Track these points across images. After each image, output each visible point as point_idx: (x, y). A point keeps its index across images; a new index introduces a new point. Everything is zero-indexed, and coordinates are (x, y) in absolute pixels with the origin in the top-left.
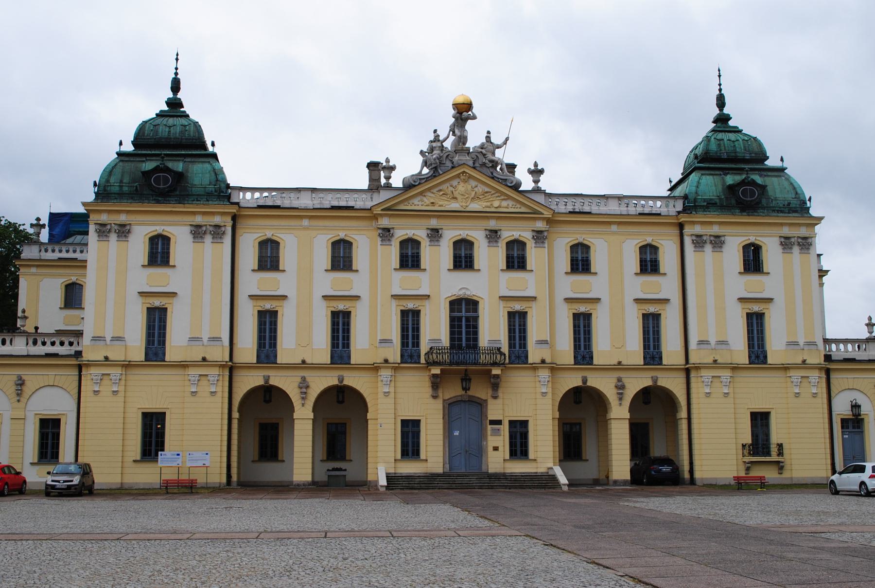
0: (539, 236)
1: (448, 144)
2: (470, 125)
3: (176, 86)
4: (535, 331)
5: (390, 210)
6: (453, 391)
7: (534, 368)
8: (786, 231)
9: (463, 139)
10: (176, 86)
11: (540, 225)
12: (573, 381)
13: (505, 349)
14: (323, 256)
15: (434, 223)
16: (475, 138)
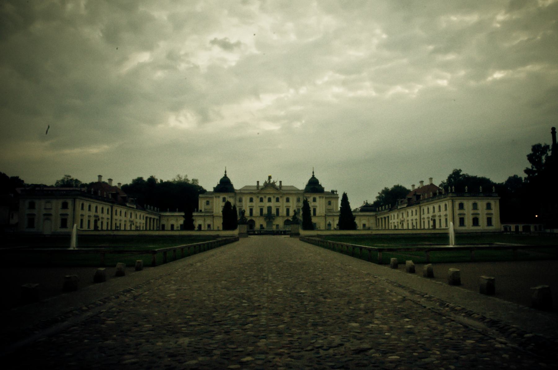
0: (281, 197)
1: (268, 182)
2: (271, 179)
3: (226, 172)
4: (280, 211)
5: (259, 193)
6: (268, 220)
7: (280, 217)
8: (320, 195)
9: (270, 182)
10: (226, 172)
11: (281, 195)
12: (286, 218)
13: (275, 214)
14: (248, 200)
15: (265, 195)
16: (272, 181)
